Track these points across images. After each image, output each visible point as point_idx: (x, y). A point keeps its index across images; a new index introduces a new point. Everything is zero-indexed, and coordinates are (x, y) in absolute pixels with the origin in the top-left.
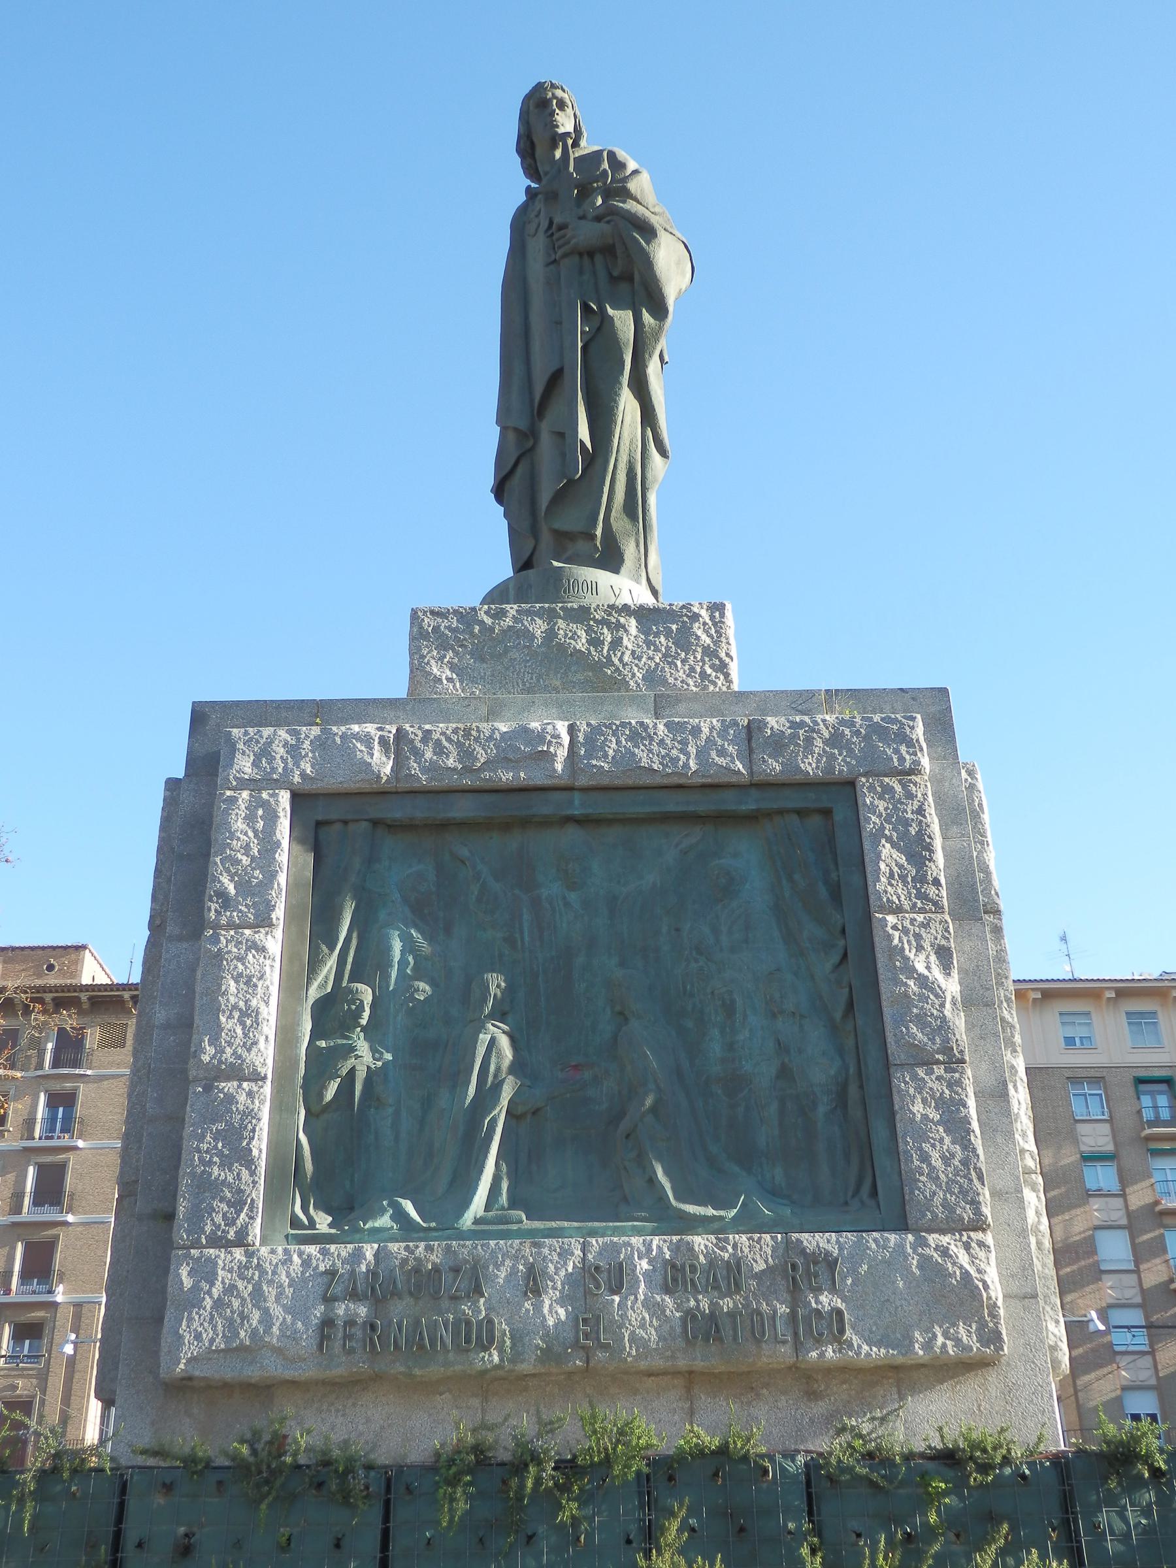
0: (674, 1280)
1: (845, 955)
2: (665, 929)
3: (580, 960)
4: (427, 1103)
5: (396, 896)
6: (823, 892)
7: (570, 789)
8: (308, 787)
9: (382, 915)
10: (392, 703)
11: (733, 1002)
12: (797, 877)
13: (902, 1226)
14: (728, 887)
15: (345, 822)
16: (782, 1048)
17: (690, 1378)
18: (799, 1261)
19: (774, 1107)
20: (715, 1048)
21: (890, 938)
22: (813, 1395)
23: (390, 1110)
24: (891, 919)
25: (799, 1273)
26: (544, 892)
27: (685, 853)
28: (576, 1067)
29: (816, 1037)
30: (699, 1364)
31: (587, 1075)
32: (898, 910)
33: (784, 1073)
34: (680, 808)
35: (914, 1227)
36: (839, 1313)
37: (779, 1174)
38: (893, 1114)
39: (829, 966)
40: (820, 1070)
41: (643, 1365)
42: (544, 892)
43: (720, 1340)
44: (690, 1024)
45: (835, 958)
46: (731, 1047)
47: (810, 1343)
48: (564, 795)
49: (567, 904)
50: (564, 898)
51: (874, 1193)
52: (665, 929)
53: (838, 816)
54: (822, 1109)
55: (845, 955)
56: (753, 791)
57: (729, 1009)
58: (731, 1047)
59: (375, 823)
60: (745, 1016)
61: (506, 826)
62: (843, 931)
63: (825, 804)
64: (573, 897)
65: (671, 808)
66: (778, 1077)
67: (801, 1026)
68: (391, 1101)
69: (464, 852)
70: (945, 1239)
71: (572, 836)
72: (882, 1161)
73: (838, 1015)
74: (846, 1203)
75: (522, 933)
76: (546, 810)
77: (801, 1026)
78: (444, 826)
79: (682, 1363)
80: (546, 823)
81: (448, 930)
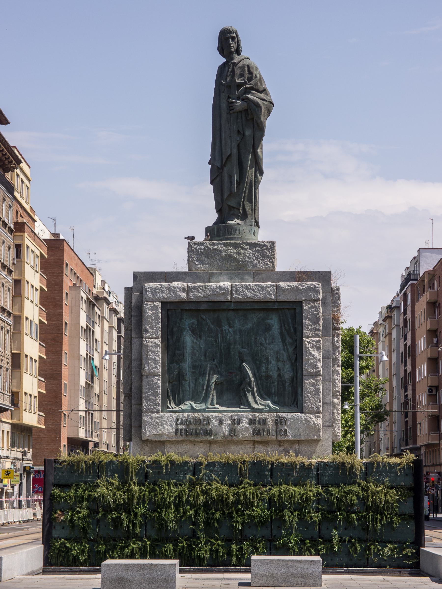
0: (251, 422)
1: (296, 347)
2: (253, 339)
3: (232, 346)
4: (197, 380)
5: (188, 328)
6: (292, 330)
7: (231, 302)
8: (165, 301)
9: (184, 333)
10: (185, 273)
11: (268, 358)
12: (286, 326)
13: (302, 411)
14: (268, 328)
15: (175, 309)
16: (279, 370)
17: (254, 442)
18: (278, 419)
19: (276, 383)
20: (264, 369)
21: (306, 344)
22: (280, 445)
23: (188, 382)
24: (307, 340)
25: (279, 421)
26: (224, 328)
27: (258, 318)
28: (231, 373)
29: (288, 367)
30: (256, 440)
31: (233, 375)
32: (308, 337)
33: (280, 375)
34: (258, 308)
35: (306, 411)
36: (286, 430)
37: (276, 399)
38: (303, 387)
39: (292, 349)
40: (288, 374)
41: (244, 439)
42: (224, 328)
43: (260, 435)
44: (258, 363)
45: (294, 347)
46: (267, 369)
47: (279, 436)
48: (229, 303)
49: (229, 332)
50: (229, 330)
51: (297, 404)
52: (253, 339)
53: (297, 311)
54: (287, 384)
55: (296, 347)
56: (277, 303)
57: (267, 359)
58: (267, 369)
59: (182, 309)
60: (271, 361)
61: (214, 311)
62: (296, 340)
63: (295, 307)
64: (231, 330)
65: (256, 307)
66: (278, 376)
67: (284, 364)
68: (188, 379)
69: (204, 317)
70: (310, 415)
71: (231, 314)
72: (299, 397)
73: (293, 361)
74: (291, 406)
75: (218, 339)
76: (225, 307)
77: (284, 364)
78: (198, 310)
79: (252, 439)
80: (224, 310)
81: (200, 337)
